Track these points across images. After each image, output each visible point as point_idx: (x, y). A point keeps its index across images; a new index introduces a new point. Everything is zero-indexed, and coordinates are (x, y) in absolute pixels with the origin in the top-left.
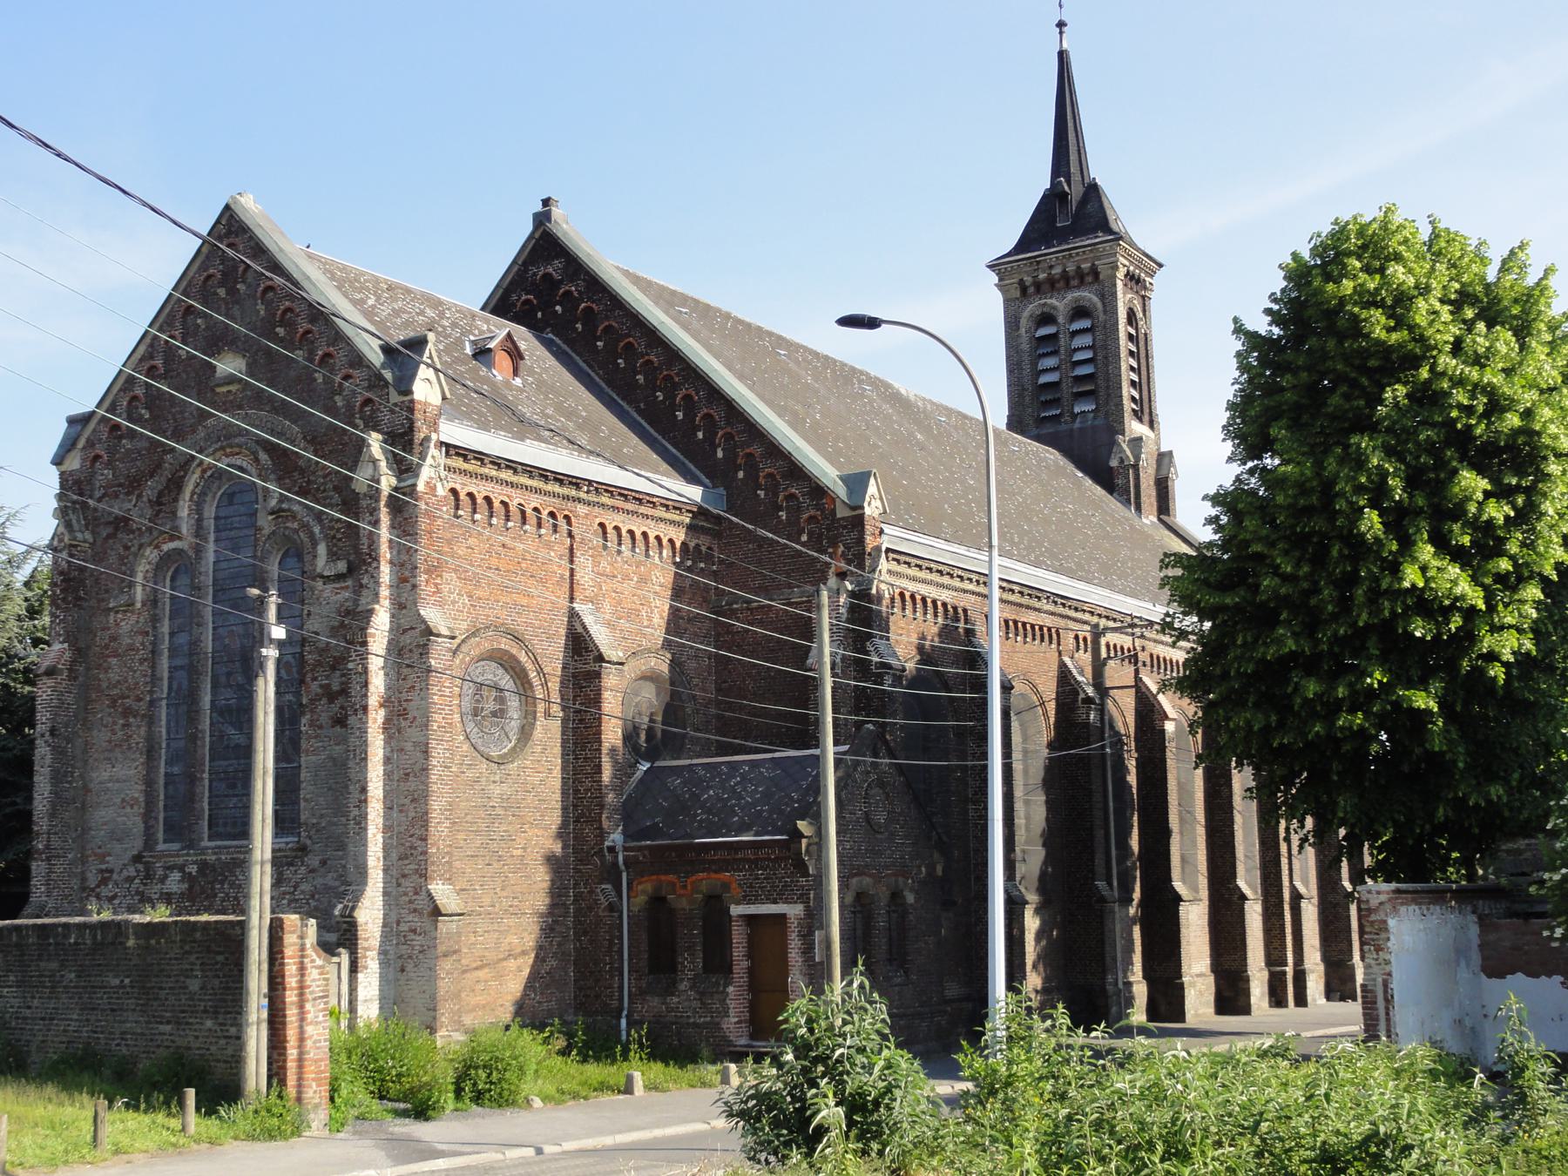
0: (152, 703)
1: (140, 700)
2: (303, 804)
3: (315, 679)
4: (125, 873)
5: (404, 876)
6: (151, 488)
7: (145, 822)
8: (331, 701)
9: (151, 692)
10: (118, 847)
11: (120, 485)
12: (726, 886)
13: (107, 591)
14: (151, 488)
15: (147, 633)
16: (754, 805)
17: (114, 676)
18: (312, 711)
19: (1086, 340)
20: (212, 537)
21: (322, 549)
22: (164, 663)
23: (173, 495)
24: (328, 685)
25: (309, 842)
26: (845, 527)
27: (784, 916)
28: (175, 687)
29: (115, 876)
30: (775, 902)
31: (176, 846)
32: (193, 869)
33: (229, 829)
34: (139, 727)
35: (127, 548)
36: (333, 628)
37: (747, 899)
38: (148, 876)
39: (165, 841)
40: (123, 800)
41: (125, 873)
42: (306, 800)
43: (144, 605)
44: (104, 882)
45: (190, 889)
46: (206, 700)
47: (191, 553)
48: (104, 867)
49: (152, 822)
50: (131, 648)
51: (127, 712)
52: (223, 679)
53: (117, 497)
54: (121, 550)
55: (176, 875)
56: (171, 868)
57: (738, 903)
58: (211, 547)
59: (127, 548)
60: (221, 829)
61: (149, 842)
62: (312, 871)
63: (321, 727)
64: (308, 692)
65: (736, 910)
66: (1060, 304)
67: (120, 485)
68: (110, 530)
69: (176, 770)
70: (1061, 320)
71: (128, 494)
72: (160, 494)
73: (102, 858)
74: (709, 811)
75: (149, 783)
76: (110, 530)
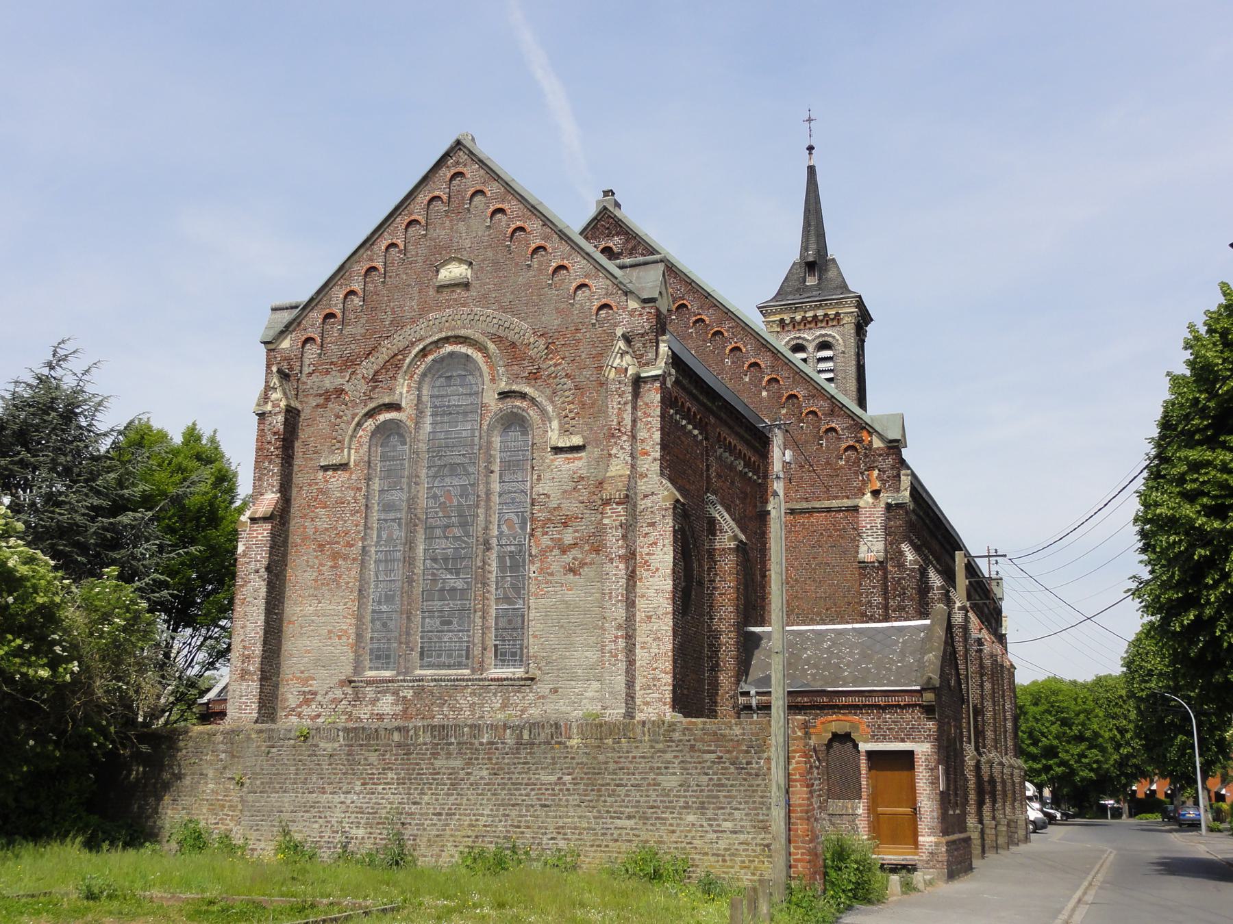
1: (352, 545)
2: (531, 640)
3: (546, 533)
4: (331, 695)
5: (646, 704)
6: (367, 368)
7: (356, 652)
8: (564, 552)
9: (363, 539)
11: (332, 363)
12: (855, 726)
14: (367, 368)
15: (359, 489)
16: (858, 662)
17: (322, 524)
18: (542, 562)
19: (830, 365)
20: (429, 412)
21: (555, 424)
22: (375, 515)
23: (391, 374)
24: (560, 539)
25: (538, 672)
26: (880, 455)
27: (910, 755)
28: (385, 536)
29: (319, 698)
30: (903, 741)
31: (387, 674)
32: (409, 694)
33: (443, 659)
36: (565, 491)
37: (874, 738)
39: (371, 669)
40: (330, 632)
41: (331, 695)
43: (356, 465)
44: (307, 702)
45: (405, 711)
48: (307, 689)
50: (341, 501)
51: (335, 556)
52: (438, 532)
53: (327, 372)
54: (333, 419)
55: (390, 698)
56: (384, 693)
57: (866, 741)
58: (429, 420)
59: (338, 417)
60: (433, 660)
61: (358, 667)
62: (543, 697)
63: (552, 574)
64: (537, 545)
65: (864, 747)
66: (810, 336)
67: (332, 363)
68: (321, 400)
69: (384, 608)
70: (811, 348)
72: (376, 373)
73: (305, 682)
74: (816, 666)
75: (360, 618)
76: (321, 400)
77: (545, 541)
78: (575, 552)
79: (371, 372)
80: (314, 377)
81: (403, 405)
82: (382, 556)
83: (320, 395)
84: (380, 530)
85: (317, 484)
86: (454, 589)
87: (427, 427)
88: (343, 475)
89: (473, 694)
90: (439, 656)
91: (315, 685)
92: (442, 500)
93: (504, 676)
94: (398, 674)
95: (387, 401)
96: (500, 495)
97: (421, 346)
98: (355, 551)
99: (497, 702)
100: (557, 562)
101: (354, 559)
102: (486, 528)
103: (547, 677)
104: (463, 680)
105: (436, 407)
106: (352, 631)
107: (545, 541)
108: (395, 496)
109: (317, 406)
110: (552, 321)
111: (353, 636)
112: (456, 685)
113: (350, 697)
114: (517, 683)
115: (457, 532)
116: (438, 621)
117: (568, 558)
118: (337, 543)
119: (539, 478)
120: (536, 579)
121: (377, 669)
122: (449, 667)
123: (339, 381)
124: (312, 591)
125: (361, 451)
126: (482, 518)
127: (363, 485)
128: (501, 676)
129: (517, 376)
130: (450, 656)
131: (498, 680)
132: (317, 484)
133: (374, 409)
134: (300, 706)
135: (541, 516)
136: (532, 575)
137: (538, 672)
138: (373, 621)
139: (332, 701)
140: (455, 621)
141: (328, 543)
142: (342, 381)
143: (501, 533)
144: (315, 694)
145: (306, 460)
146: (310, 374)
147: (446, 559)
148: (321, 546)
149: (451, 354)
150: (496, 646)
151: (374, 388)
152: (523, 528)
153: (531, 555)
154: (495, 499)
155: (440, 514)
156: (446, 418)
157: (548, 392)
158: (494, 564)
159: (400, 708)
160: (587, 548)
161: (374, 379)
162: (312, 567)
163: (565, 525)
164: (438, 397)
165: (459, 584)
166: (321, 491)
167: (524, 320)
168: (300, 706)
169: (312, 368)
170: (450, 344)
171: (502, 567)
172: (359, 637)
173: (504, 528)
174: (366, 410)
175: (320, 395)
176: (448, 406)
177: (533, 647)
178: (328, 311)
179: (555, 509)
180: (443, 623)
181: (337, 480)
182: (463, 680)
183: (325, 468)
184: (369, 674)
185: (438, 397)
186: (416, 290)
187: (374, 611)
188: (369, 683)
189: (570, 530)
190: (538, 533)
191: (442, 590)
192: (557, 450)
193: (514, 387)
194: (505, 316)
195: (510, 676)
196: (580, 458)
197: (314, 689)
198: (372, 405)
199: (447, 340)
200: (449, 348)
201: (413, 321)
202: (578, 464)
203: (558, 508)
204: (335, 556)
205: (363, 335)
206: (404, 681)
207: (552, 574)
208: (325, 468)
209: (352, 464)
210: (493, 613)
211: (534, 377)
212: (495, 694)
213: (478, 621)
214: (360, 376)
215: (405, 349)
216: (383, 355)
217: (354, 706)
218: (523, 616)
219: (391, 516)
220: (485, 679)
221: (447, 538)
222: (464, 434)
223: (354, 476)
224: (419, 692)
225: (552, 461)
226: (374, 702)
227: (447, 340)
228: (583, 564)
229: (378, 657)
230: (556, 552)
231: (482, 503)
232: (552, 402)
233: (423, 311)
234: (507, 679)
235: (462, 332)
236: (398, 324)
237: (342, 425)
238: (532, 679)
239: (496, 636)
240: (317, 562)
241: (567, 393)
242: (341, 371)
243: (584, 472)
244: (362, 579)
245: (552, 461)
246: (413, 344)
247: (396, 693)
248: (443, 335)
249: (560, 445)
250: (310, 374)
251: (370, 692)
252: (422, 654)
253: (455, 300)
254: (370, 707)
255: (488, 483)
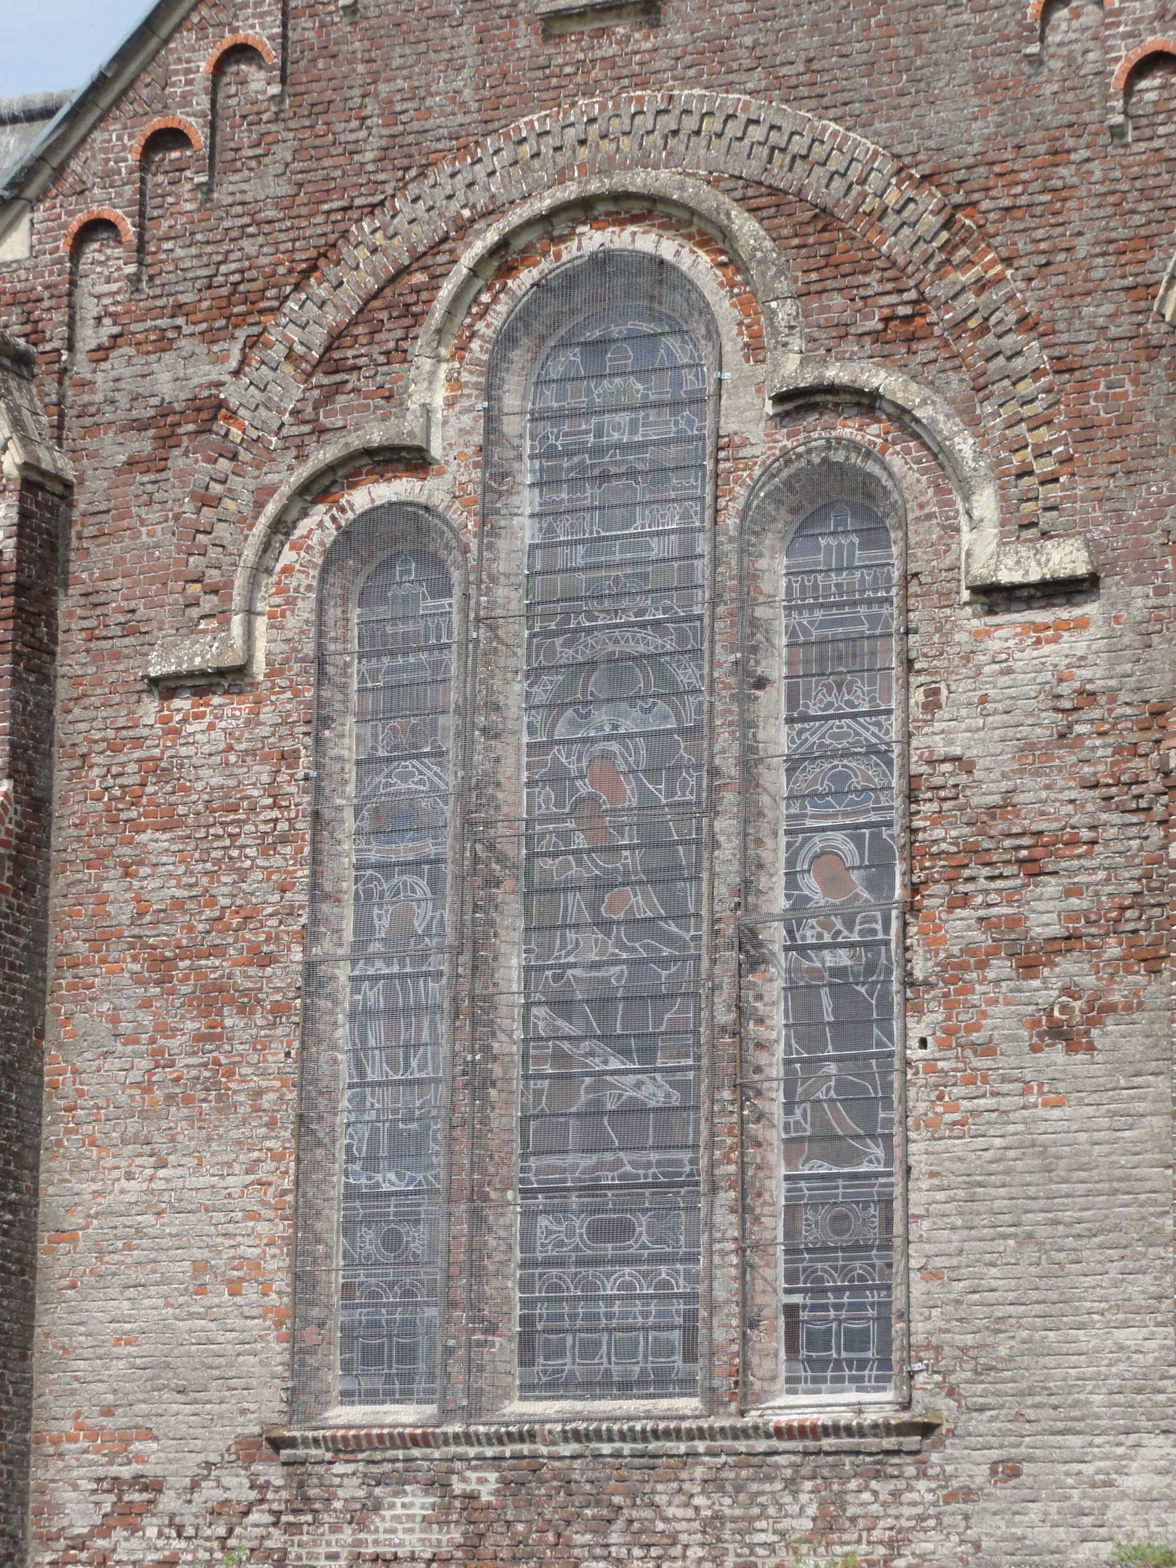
0: (313, 977)
1: (269, 960)
2: (918, 1288)
3: (965, 900)
4: (209, 1493)
6: (304, 322)
7: (292, 1338)
8: (1028, 967)
9: (308, 936)
10: (179, 1413)
11: (178, 309)
13: (129, 630)
15: (288, 758)
17: (160, 888)
18: (950, 1006)
20: (526, 472)
21: (986, 502)
22: (346, 852)
24: (1014, 922)
25: (945, 1405)
28: (383, 923)
29: (169, 1501)
31: (406, 1415)
32: (485, 1485)
33: (601, 1362)
34: (260, 1045)
35: (205, 501)
36: (1028, 747)
38: (302, 1502)
39: (347, 1397)
40: (200, 1267)
41: (209, 1493)
42: (932, 1275)
44: (128, 1516)
46: (512, 966)
47: (456, 516)
48: (126, 1472)
49: (311, 1336)
51: (212, 999)
52: (575, 904)
53: (164, 343)
54: (188, 506)
56: (399, 1482)
58: (527, 501)
60: (568, 1364)
61: (300, 1395)
62: (968, 1494)
63: (987, 1049)
64: (933, 944)
67: (178, 309)
68: (143, 444)
69: (388, 1180)
71: (210, 337)
72: (336, 338)
76: (143, 444)
77: (961, 928)
78: (1069, 967)
79: (318, 336)
80: (116, 363)
81: (436, 450)
82: (374, 996)
83: (140, 426)
84: (364, 900)
85: (138, 742)
86: (633, 1110)
87: (522, 528)
88: (228, 711)
89: (713, 1483)
90: (589, 1350)
91: (153, 1457)
92: (584, 788)
93: (824, 1419)
94: (446, 1414)
95: (376, 436)
96: (793, 765)
97: (492, 237)
98: (282, 978)
99: (802, 1511)
100: (1004, 1005)
101: (278, 1010)
102: (746, 888)
103: (978, 1422)
104: (677, 1435)
105: (551, 453)
106: (276, 1264)
107: (961, 928)
108: (415, 781)
109: (131, 463)
110: (961, 124)
111: (281, 1282)
112: (653, 1453)
113: (277, 1499)
114: (871, 1443)
115: (640, 902)
116: (580, 1224)
117: (1045, 989)
118: (216, 951)
119: (932, 703)
120: (930, 1066)
121: (371, 1397)
122: (625, 1388)
123: (204, 373)
124: (132, 1126)
125: (292, 622)
126: (728, 849)
127: (302, 743)
128: (811, 1417)
129: (842, 330)
130: (627, 1351)
131: (802, 1432)
132: (138, 742)
133: (331, 468)
134: (104, 1530)
135: (943, 836)
136: (915, 1053)
137: (945, 1405)
138: (349, 1227)
139: (215, 1513)
140: (642, 1224)
141: (183, 952)
142: (215, 373)
143: (799, 903)
144: (155, 1486)
145: (98, 658)
146: (101, 353)
147: (603, 1003)
148: (161, 967)
149: (603, 261)
150: (791, 1311)
151: (330, 394)
152: (879, 882)
153: (908, 981)
154: (776, 780)
155: (580, 841)
156: (590, 494)
157: (957, 383)
158: (778, 1017)
159: (456, 1534)
160: (1113, 949)
161: (331, 361)
162: (132, 1040)
163: (1033, 869)
164: (557, 417)
165: (654, 1092)
166: (154, 769)
167: (862, 124)
168: (104, 1530)
169: (110, 327)
170: (597, 223)
171: (804, 1024)
172: (303, 1282)
173: (810, 885)
174: (304, 472)
175: (140, 426)
176: (598, 451)
177: (925, 1312)
178: (157, 122)
179: (991, 810)
180: (598, 1232)
181: (208, 730)
182: (677, 1435)
183: (165, 687)
184: (345, 1416)
185: (557, 417)
186: (466, 35)
187: (351, 1193)
188: (345, 1446)
189: (1051, 887)
190: (934, 899)
191: (594, 1112)
192: (995, 597)
193: (835, 373)
194: (793, 116)
195: (846, 1418)
196: (1082, 624)
197: (149, 1469)
198: (323, 455)
199: (584, 209)
200: (593, 239)
201: (463, 146)
202: (1076, 644)
203: (1006, 806)
204: (212, 999)
205: (285, 204)
206: (468, 1439)
207: (987, 1049)
208: (165, 687)
209: (260, 667)
210: (778, 1191)
211: (901, 333)
212: (792, 1485)
213: (726, 1220)
214: (277, 353)
215: (435, 248)
216: (359, 271)
217: (293, 1529)
218: (887, 1202)
219: (404, 851)
220: (756, 1432)
221: (604, 925)
222: (657, 548)
223: (268, 714)
224: (522, 1477)
225: (979, 636)
226: (361, 1515)
227: (584, 209)
228: (1099, 1010)
229: (372, 1356)
230: (1000, 967)
231: (729, 798)
232: (974, 423)
233: (495, 112)
234: (834, 1430)
235: (638, 180)
236: (409, 160)
237: (222, 531)
238: (926, 1429)
239: (791, 1276)
240: (146, 1019)
241: (1026, 388)
242: (210, 337)
243: (1096, 675)
244: (307, 1081)
245: (979, 636)
246: (463, 228)
247: (438, 1484)
248: (570, 191)
249: (1007, 576)
250: (101, 353)
251: (346, 1480)
252: (526, 1344)
253: (610, 62)
254: (347, 1534)
255: (747, 724)
